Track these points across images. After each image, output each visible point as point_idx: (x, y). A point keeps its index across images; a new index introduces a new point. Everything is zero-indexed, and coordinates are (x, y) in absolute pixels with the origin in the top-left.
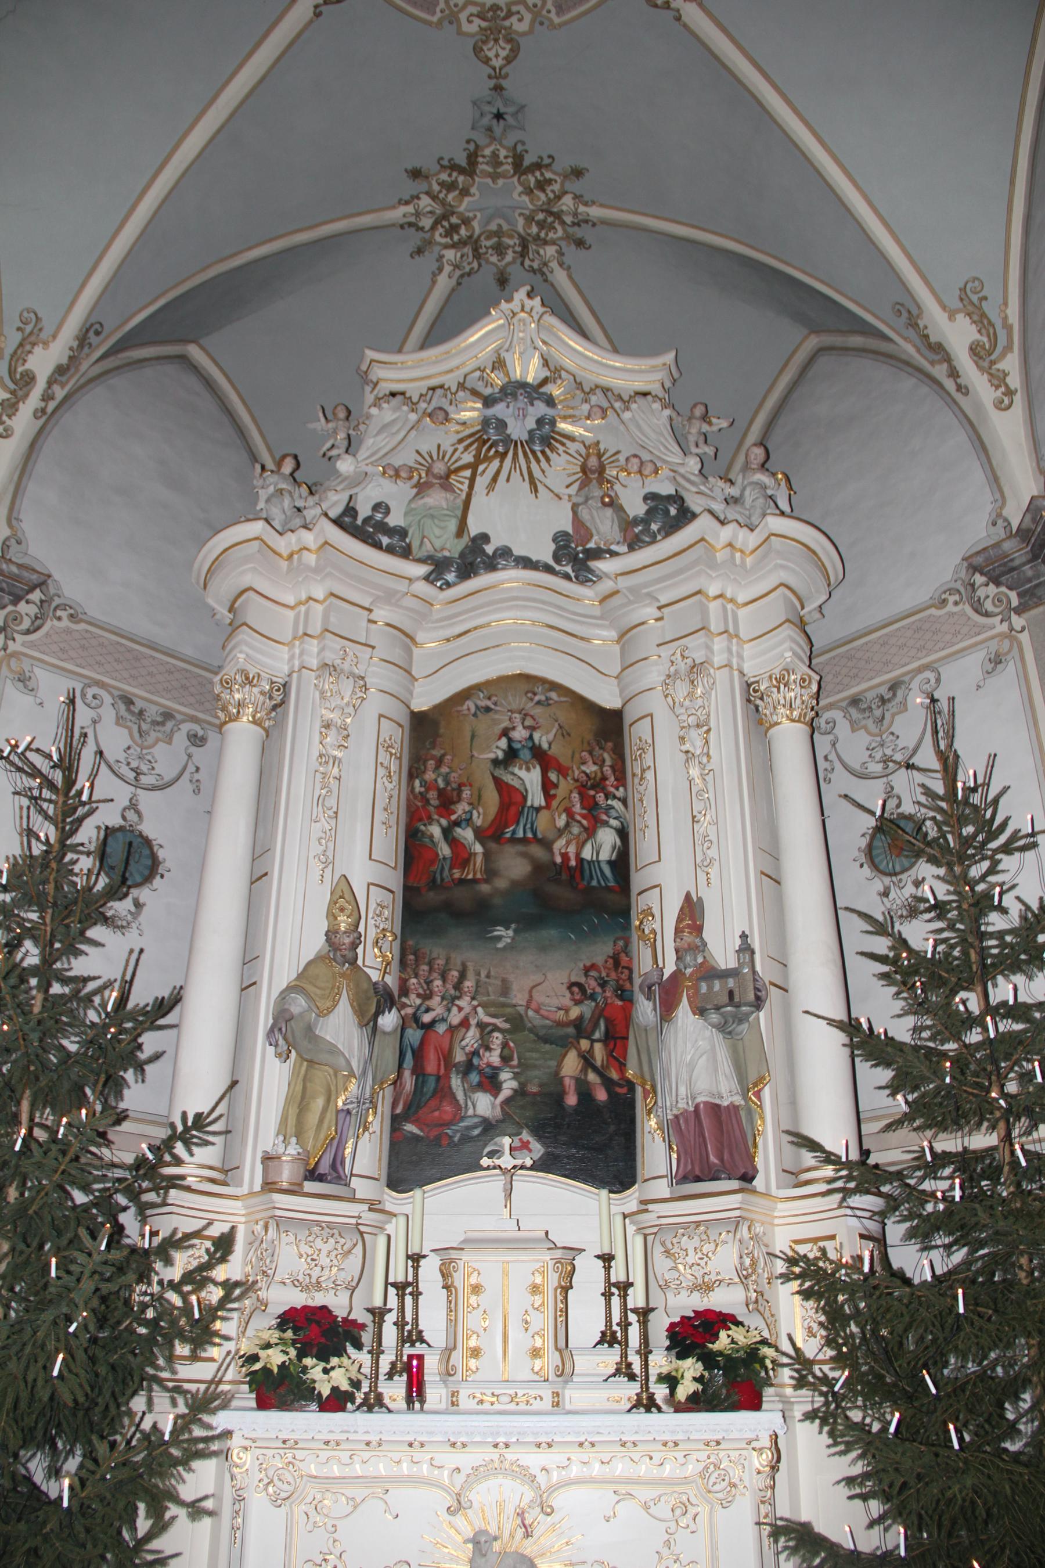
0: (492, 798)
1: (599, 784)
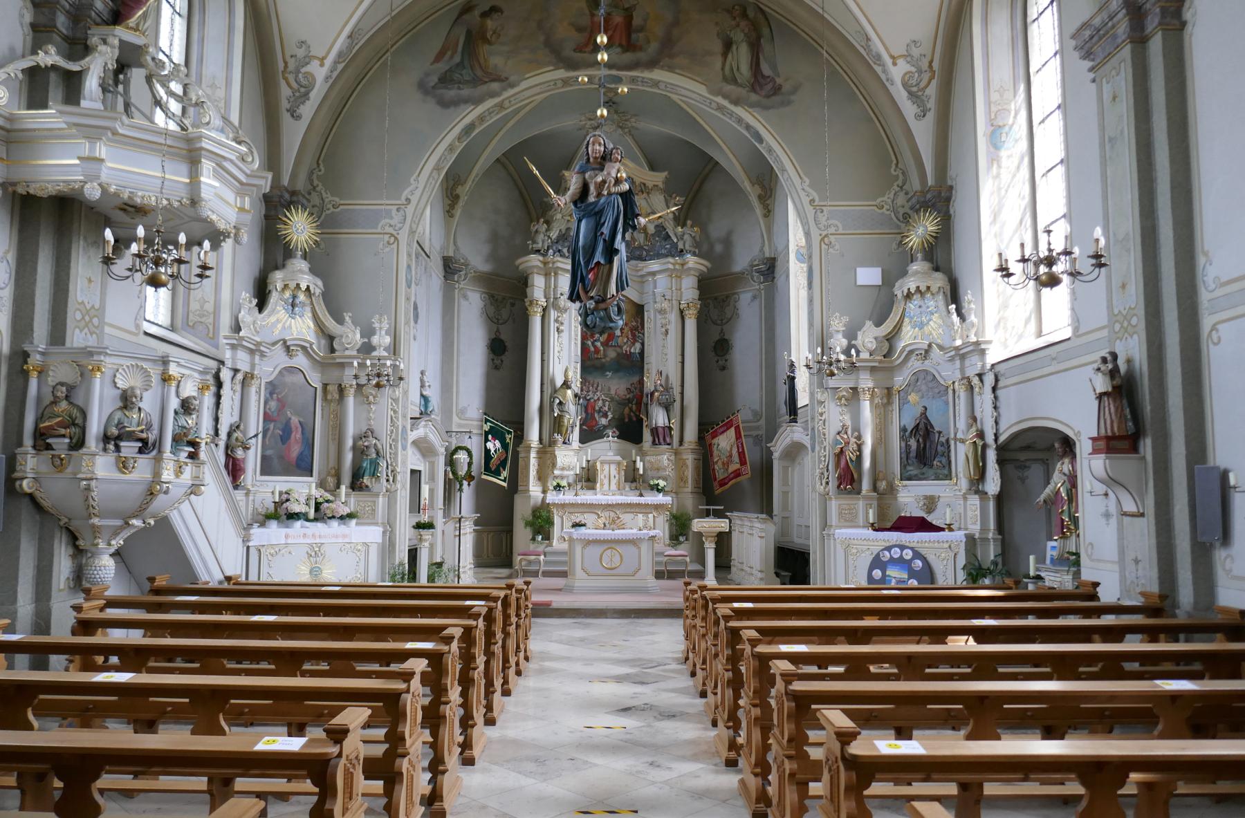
1: (636, 328)
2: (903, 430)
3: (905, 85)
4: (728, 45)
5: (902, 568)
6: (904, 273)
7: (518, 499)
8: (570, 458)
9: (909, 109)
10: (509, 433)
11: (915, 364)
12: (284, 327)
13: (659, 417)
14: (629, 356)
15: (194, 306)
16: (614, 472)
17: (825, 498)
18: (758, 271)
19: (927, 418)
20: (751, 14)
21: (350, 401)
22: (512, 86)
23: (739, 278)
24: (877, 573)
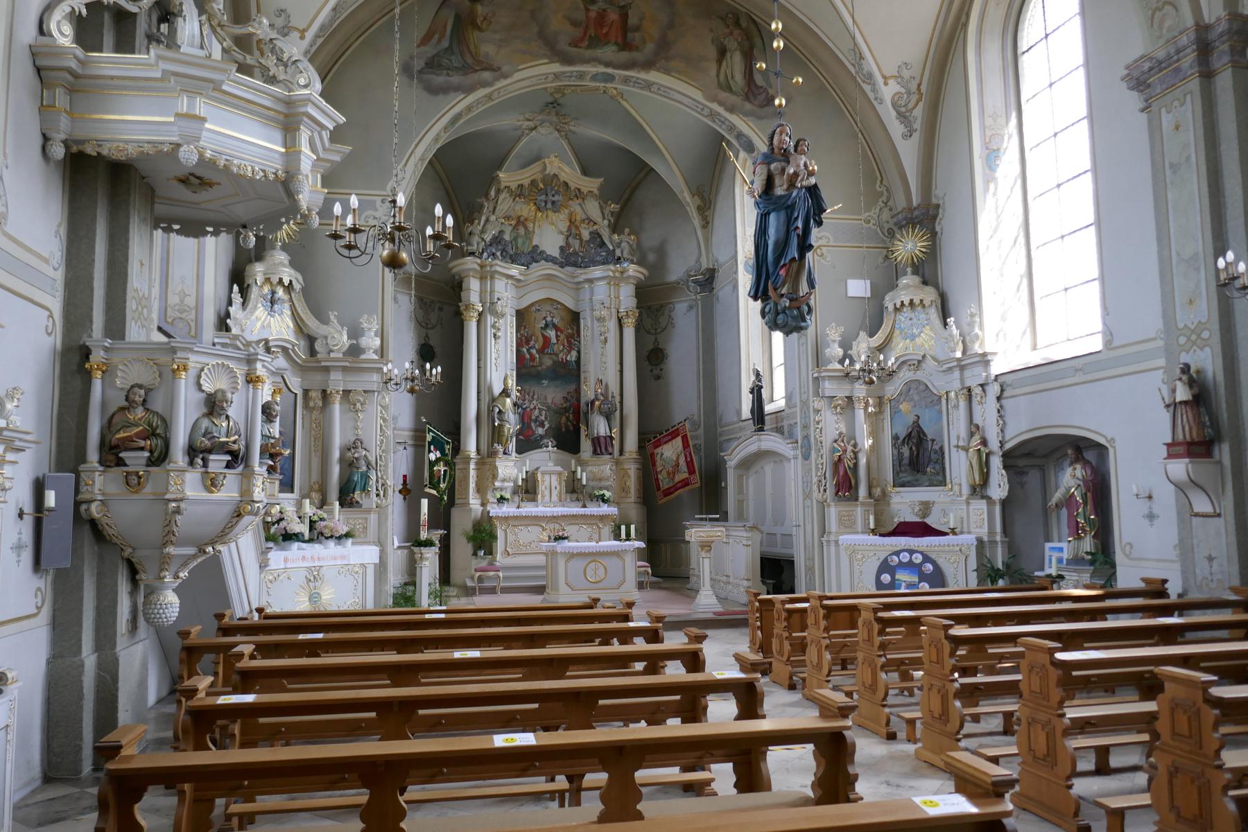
0: (541, 340)
2: (895, 438)
3: (894, 105)
4: (722, 53)
5: (912, 572)
6: (893, 286)
7: (455, 513)
8: (509, 468)
9: (896, 128)
10: (448, 443)
11: (905, 375)
12: (263, 327)
13: (600, 427)
14: (565, 364)
15: (173, 300)
16: (555, 483)
17: (822, 505)
18: (695, 282)
19: (919, 426)
20: (744, 25)
21: (336, 407)
22: (505, 76)
23: (673, 289)
24: (886, 578)
